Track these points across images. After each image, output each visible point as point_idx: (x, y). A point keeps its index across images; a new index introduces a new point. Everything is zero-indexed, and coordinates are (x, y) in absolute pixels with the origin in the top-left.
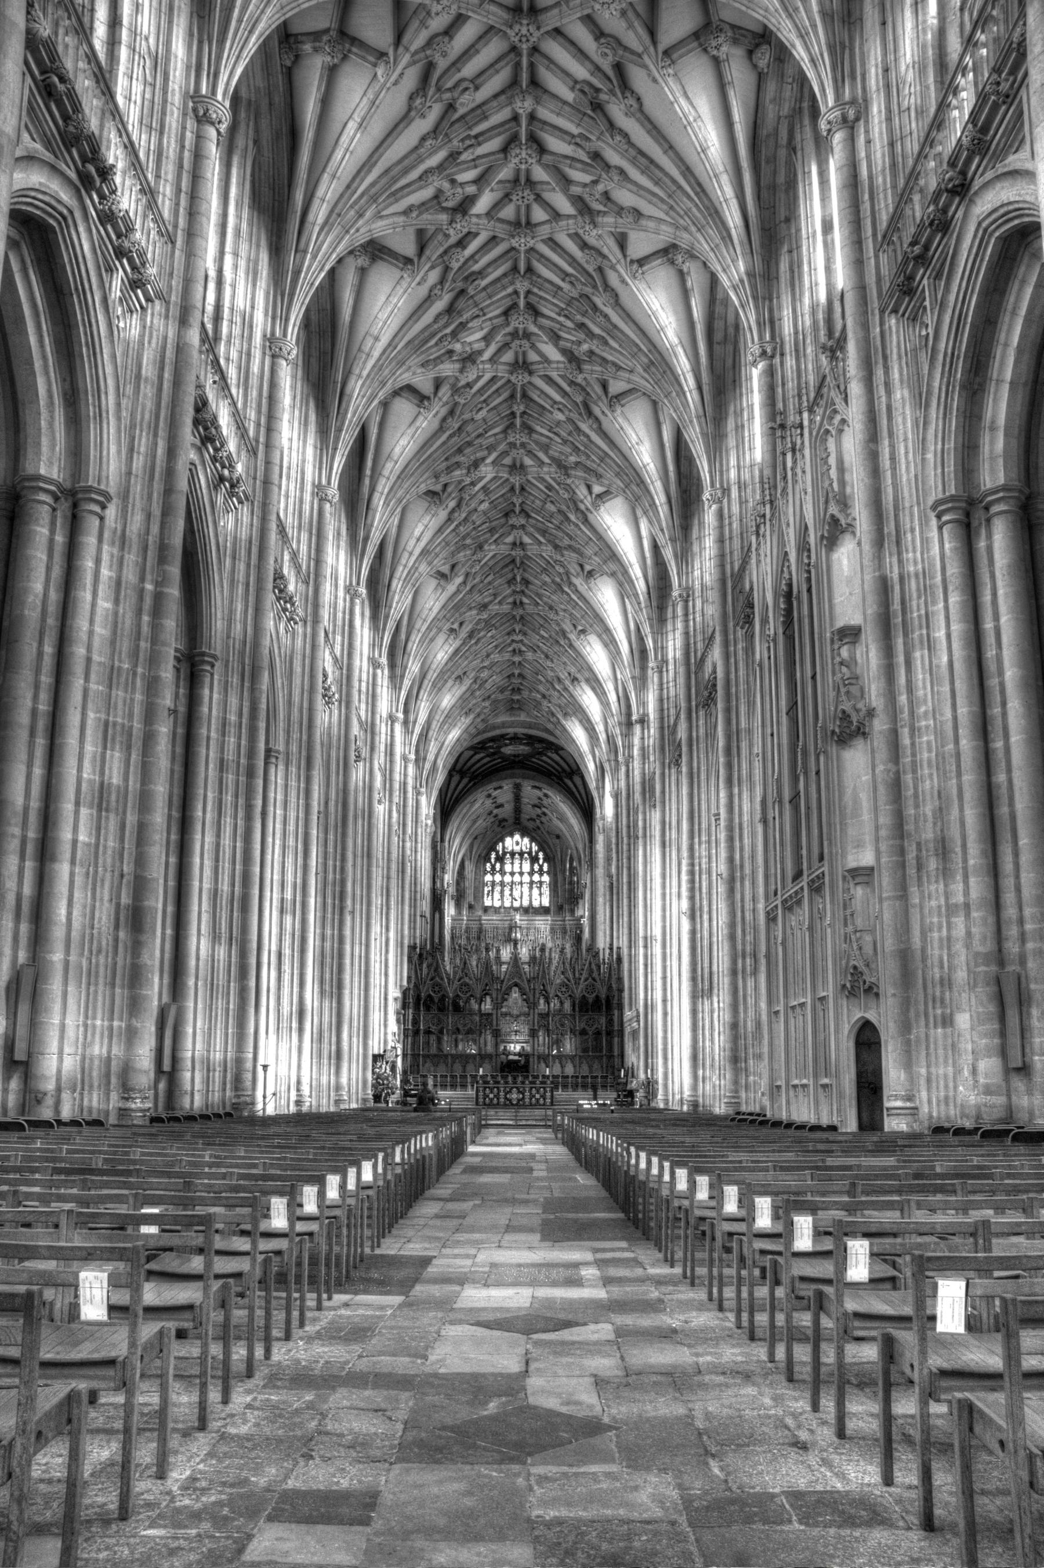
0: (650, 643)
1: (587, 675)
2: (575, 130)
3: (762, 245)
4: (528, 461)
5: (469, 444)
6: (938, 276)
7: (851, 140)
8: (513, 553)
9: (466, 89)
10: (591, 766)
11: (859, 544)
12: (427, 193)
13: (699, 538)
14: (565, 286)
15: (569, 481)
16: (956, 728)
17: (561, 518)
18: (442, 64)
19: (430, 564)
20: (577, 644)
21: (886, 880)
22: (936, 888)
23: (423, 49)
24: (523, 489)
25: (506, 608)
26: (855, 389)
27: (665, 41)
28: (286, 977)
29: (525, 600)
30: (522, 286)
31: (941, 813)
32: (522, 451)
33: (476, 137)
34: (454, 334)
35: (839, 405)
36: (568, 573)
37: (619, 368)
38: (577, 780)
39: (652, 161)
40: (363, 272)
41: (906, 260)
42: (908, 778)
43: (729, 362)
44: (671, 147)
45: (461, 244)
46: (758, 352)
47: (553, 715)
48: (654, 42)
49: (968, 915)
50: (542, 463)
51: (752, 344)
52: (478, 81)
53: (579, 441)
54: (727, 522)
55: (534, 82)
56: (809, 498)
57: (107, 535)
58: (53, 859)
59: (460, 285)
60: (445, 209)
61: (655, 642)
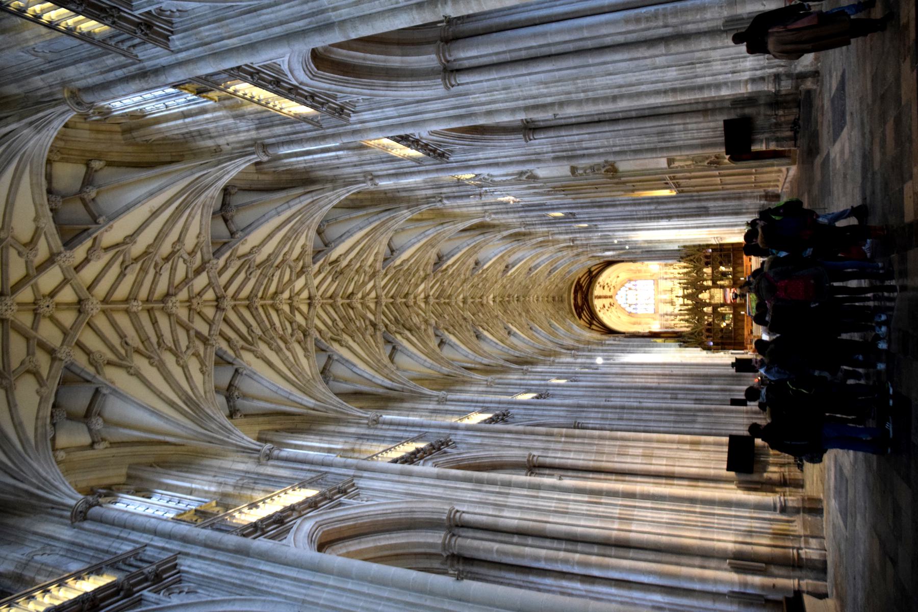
0: (541, 239)
4: (461, 296)
6: (440, 145)
7: (378, 177)
8: (498, 301)
14: (400, 281)
16: (614, 131)
19: (507, 339)
21: (673, 154)
22: (676, 136)
25: (519, 304)
28: (706, 397)
29: (516, 296)
30: (399, 300)
31: (646, 135)
34: (419, 328)
38: (592, 269)
39: (361, 249)
41: (434, 157)
42: (633, 147)
45: (386, 326)
46: (440, 203)
48: (323, 251)
49: (688, 123)
55: (331, 297)
57: (544, 455)
58: (673, 473)
59: (401, 326)
60: (375, 332)
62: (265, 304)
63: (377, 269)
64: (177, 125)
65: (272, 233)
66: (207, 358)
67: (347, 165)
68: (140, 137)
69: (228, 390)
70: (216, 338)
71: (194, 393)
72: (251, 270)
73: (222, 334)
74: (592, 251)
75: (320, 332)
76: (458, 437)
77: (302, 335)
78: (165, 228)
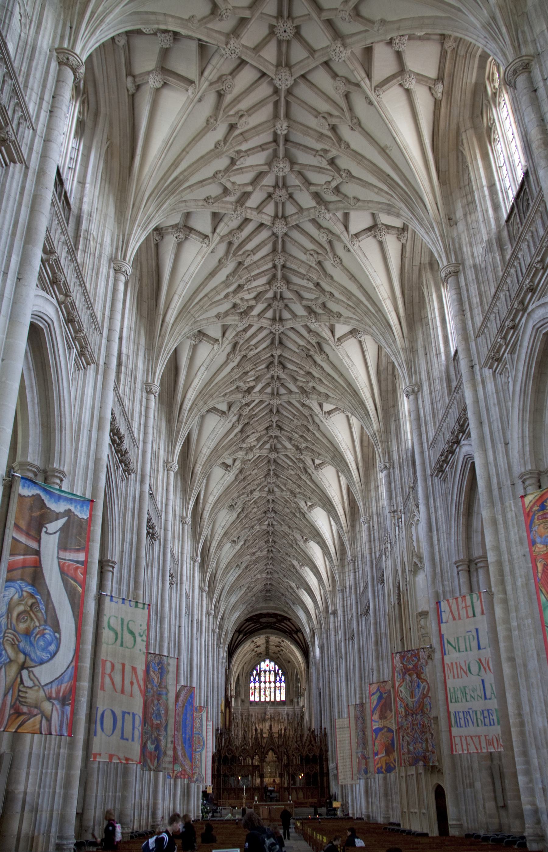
0: (337, 578)
1: (306, 586)
2: (298, 362)
3: (383, 417)
4: (276, 489)
5: (249, 484)
8: (268, 529)
9: (252, 349)
10: (308, 630)
11: (426, 576)
13: (359, 531)
14: (296, 421)
15: (296, 500)
17: (292, 515)
20: (301, 571)
24: (273, 501)
25: (264, 553)
26: (422, 508)
27: (338, 335)
29: (273, 550)
30: (275, 419)
32: (273, 485)
33: (255, 365)
34: (243, 441)
35: (416, 513)
36: (296, 540)
37: (320, 454)
38: (299, 634)
39: (333, 378)
43: (371, 456)
44: (342, 375)
46: (383, 467)
47: (287, 603)
48: (333, 336)
50: (282, 491)
51: (379, 463)
52: (257, 346)
53: (301, 483)
54: (372, 532)
55: (281, 343)
59: (246, 421)
61: (340, 577)
62: (276, 270)
63: (310, 396)
64: (480, 178)
65: (356, 279)
66: (221, 205)
67: (429, 364)
68: (467, 138)
69: (185, 226)
70: (243, 214)
71: (186, 189)
72: (315, 256)
73: (246, 221)
74: (321, 634)
75: (245, 330)
77: (242, 310)
78: (366, 162)
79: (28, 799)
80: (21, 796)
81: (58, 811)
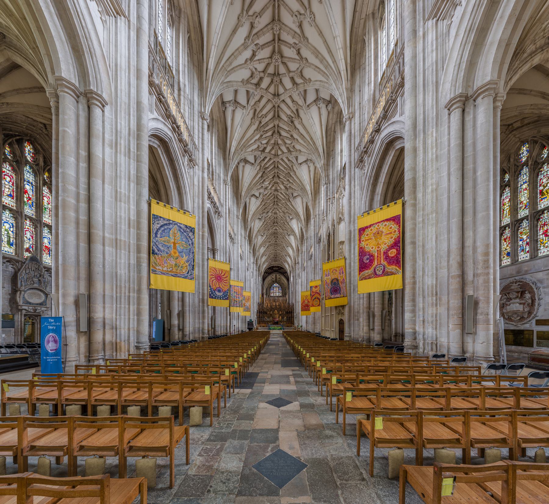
2: (287, 129)
12: (255, 147)
18: (258, 110)
23: (254, 105)
26: (347, 187)
30: (276, 171)
34: (263, 182)
40: (244, 166)
45: (264, 160)
51: (323, 182)
56: (335, 214)
59: (264, 170)
76: (197, 171)
79: (107, 321)
80: (100, 320)
81: (134, 328)
